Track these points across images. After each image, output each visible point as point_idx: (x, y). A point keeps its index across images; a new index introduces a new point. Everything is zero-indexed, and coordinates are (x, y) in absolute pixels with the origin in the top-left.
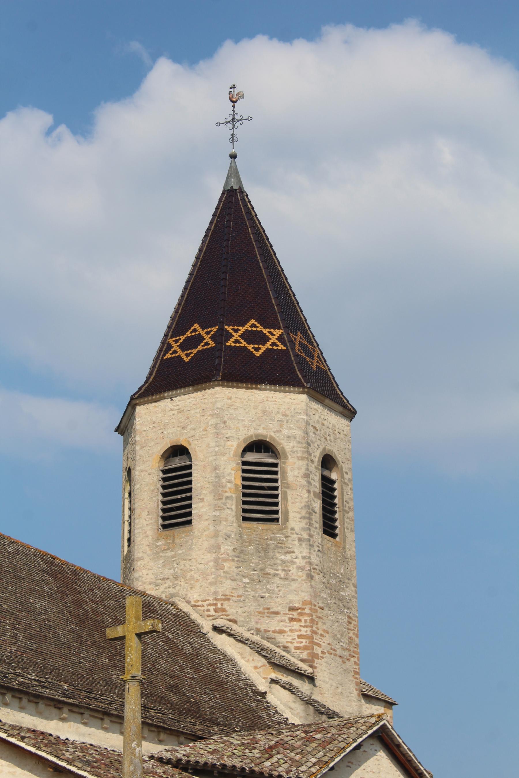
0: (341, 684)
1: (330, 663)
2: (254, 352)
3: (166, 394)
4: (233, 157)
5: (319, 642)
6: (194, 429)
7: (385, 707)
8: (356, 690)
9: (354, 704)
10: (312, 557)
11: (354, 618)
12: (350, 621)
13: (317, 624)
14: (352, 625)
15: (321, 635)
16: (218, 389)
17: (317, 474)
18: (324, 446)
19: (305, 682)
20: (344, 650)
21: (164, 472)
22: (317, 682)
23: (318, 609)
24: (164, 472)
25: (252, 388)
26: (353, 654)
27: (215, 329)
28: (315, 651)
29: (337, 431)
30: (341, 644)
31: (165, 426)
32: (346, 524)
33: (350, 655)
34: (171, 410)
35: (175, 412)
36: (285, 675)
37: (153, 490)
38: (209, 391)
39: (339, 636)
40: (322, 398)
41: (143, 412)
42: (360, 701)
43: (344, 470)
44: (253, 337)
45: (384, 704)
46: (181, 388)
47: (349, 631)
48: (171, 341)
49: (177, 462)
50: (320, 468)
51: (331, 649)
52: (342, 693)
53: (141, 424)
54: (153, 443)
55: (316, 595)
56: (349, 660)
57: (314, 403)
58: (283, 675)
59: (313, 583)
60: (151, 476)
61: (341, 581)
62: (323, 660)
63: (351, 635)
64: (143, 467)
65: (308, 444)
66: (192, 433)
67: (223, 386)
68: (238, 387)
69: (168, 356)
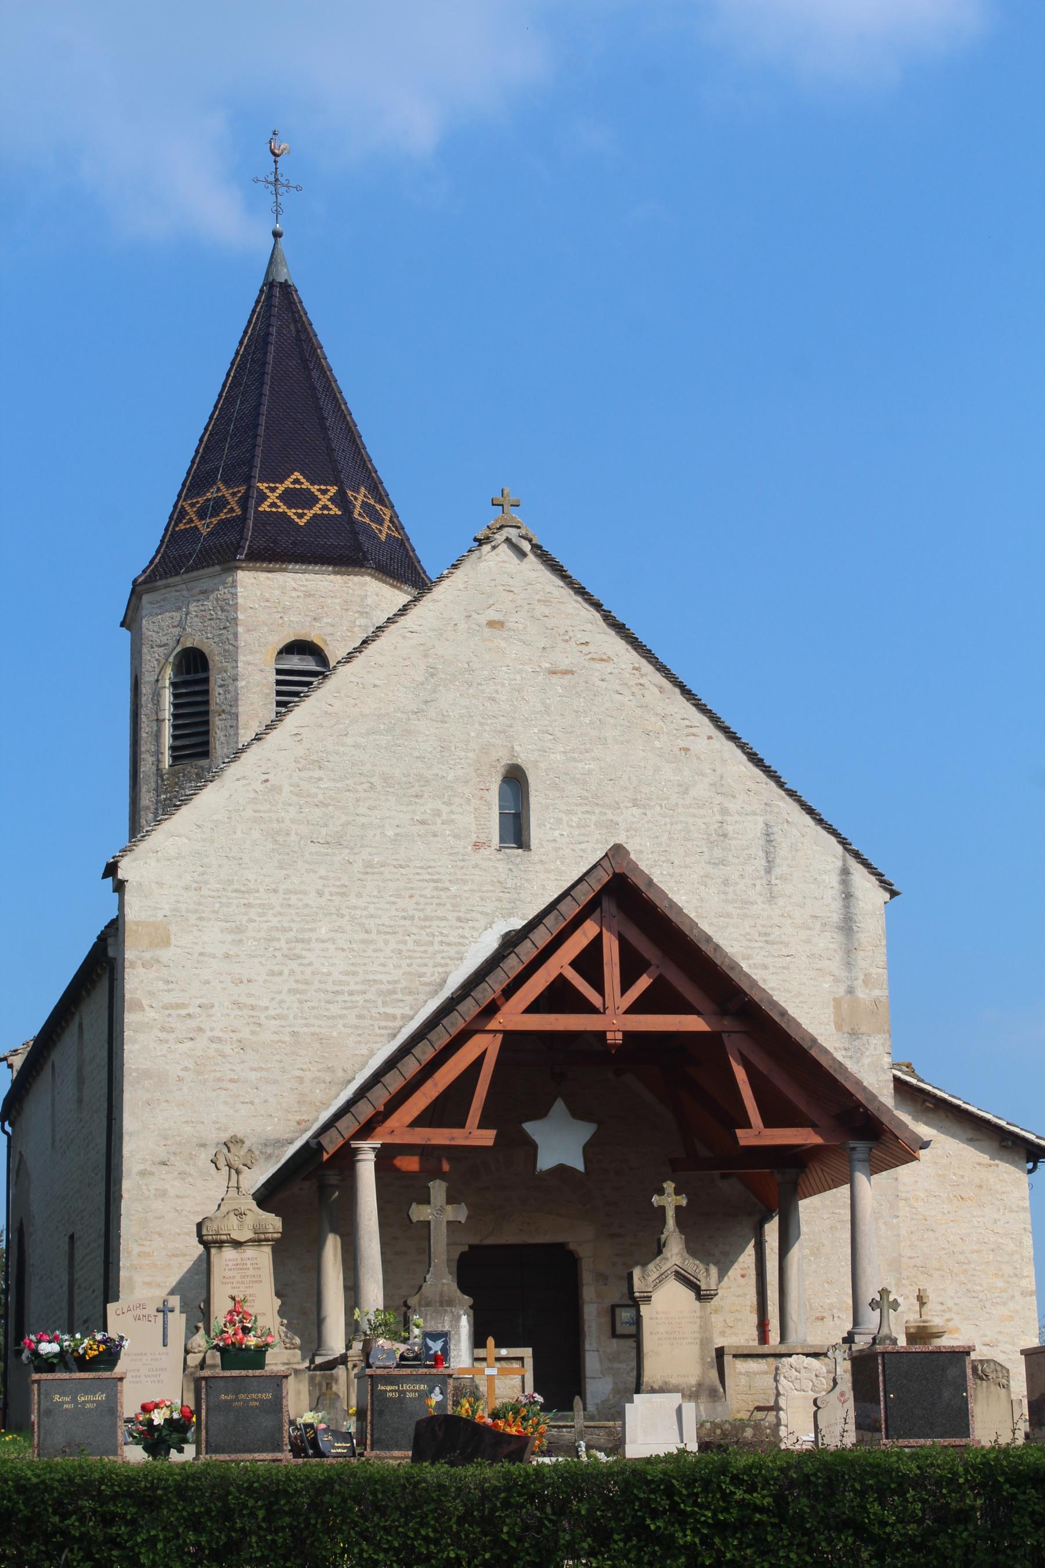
2: (297, 520)
3: (291, 567)
4: (277, 235)
6: (333, 626)
16: (367, 578)
21: (279, 672)
24: (279, 672)
25: (395, 587)
27: (333, 490)
31: (286, 610)
34: (295, 589)
35: (301, 594)
37: (267, 695)
38: (356, 579)
41: (246, 580)
44: (298, 498)
46: (316, 563)
48: (262, 486)
49: (295, 662)
53: (245, 598)
54: (266, 629)
60: (263, 674)
64: (250, 658)
66: (330, 630)
67: (373, 576)
68: (385, 582)
69: (265, 507)
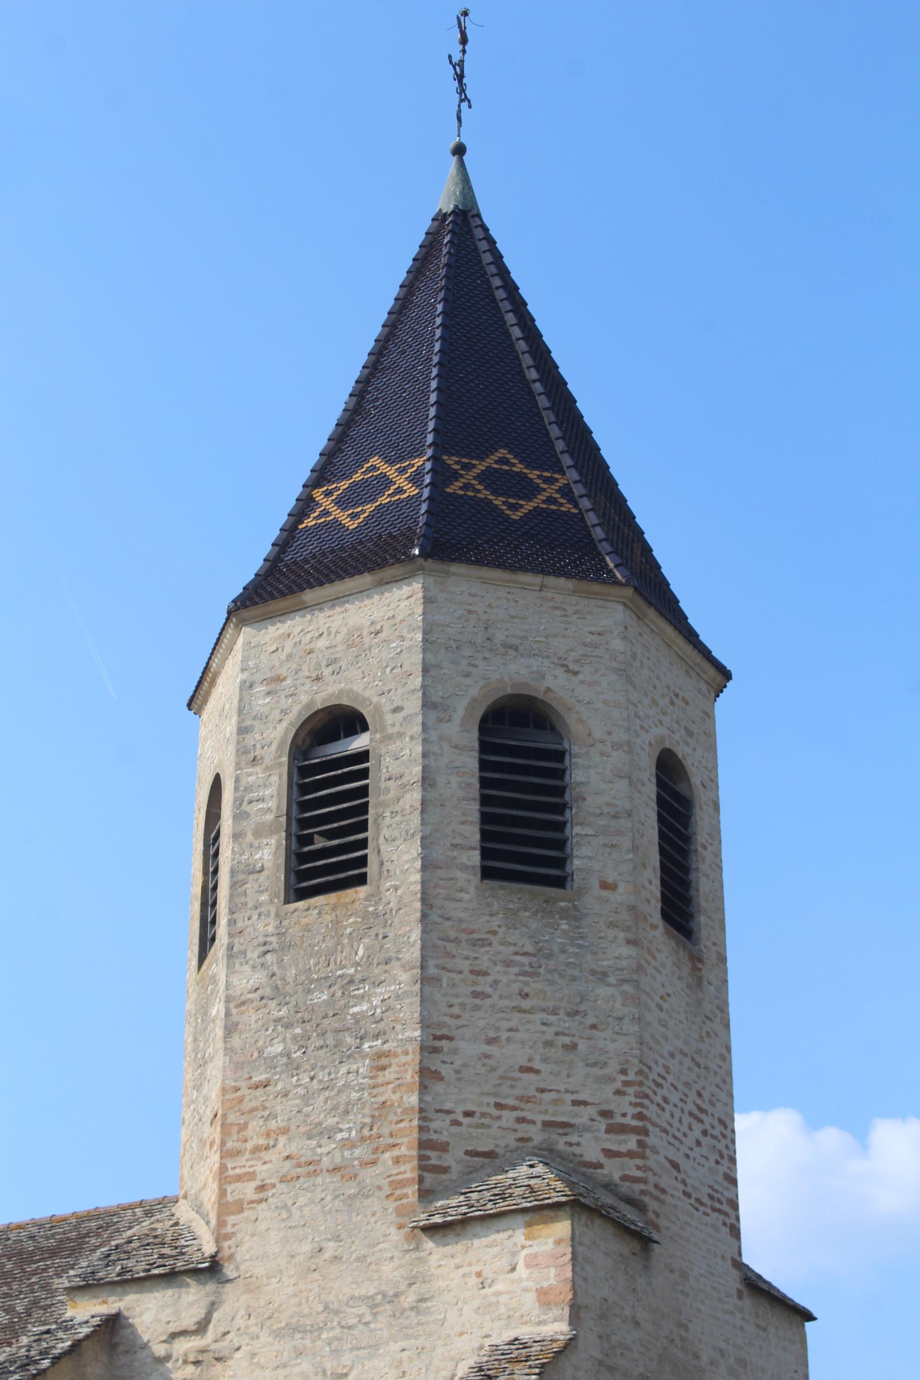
0: (337, 1238)
1: (290, 1203)
4: (459, 150)
5: (247, 1170)
7: (529, 1225)
8: (400, 1227)
9: (387, 1268)
10: (235, 981)
11: (399, 1050)
12: (384, 1061)
13: (244, 1127)
14: (394, 1068)
15: (256, 1149)
17: (274, 779)
18: (304, 699)
19: (188, 1285)
20: (353, 1146)
22: (229, 1271)
23: (247, 1092)
26: (391, 1141)
28: (230, 1198)
29: (365, 633)
30: (339, 1136)
32: (385, 832)
33: (375, 1151)
36: (111, 1299)
39: (331, 1121)
40: (290, 601)
42: (417, 1248)
43: (387, 708)
45: (520, 1219)
47: (375, 1092)
50: (285, 759)
51: (299, 1165)
52: (336, 1258)
55: (238, 1063)
56: (374, 1163)
57: (279, 625)
58: (105, 1302)
59: (236, 1041)
61: (351, 982)
62: (264, 1205)
63: (387, 1094)
65: (243, 730)
